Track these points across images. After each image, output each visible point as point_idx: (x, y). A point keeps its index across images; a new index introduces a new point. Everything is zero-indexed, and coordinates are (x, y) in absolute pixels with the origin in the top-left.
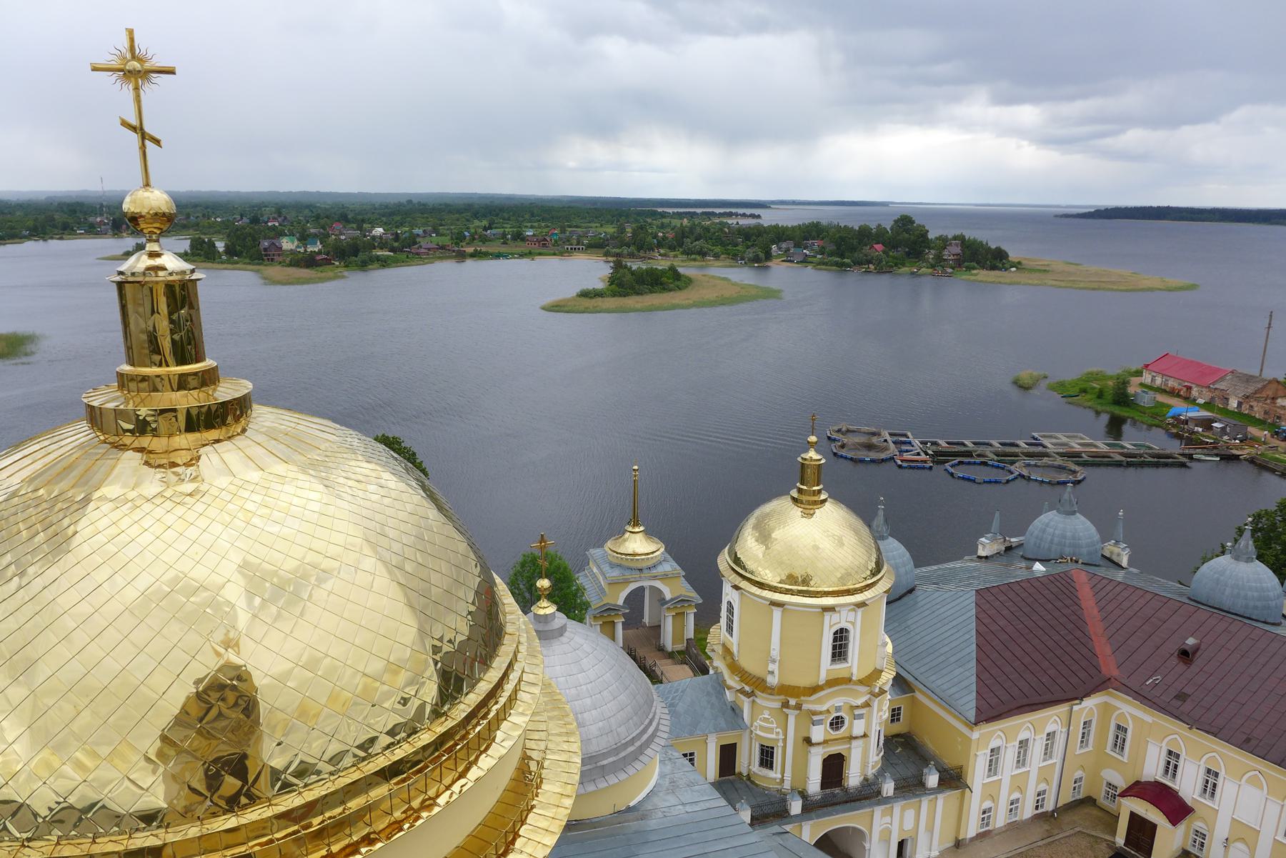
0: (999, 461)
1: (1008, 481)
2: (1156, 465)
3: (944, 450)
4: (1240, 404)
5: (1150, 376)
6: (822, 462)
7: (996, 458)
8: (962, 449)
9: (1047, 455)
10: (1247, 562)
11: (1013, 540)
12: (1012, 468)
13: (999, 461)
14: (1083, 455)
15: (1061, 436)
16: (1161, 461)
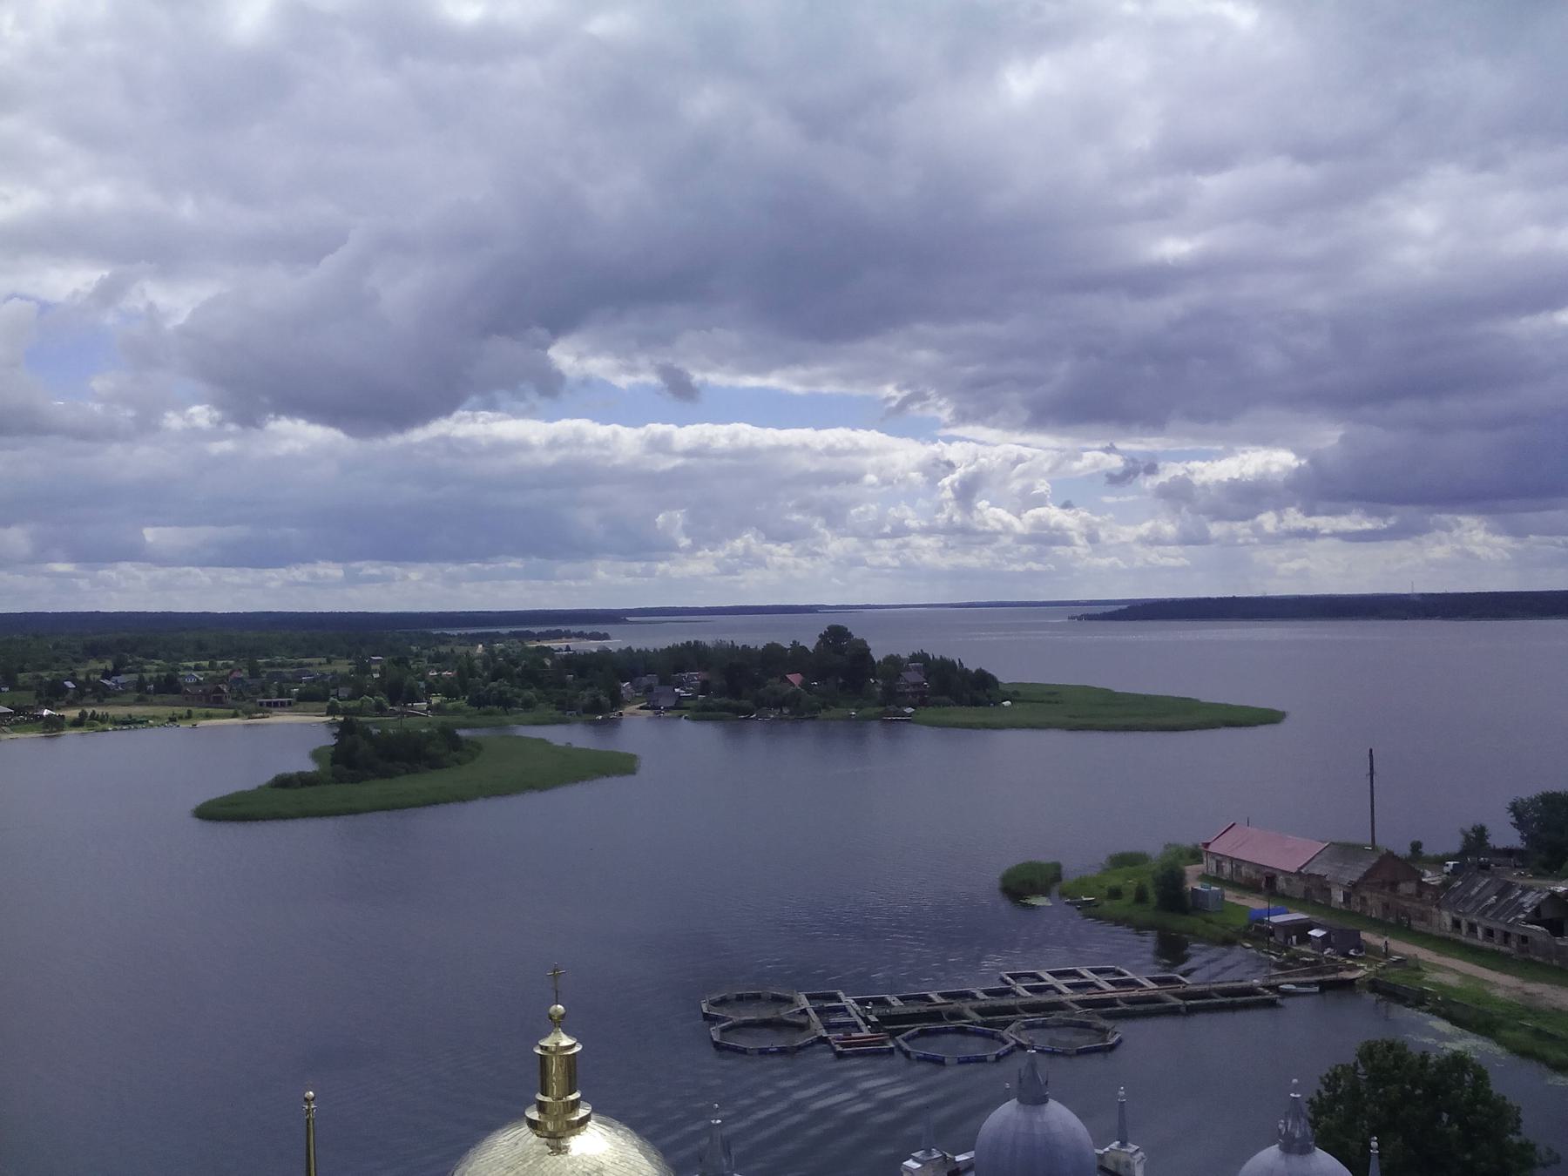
0: (985, 1024)
1: (998, 1058)
2: (1233, 1007)
3: (894, 1011)
4: (1347, 897)
5: (1214, 862)
6: (577, 1049)
7: (978, 1018)
8: (923, 1008)
9: (1059, 1006)
10: (1301, 1154)
11: (959, 1158)
12: (1005, 1034)
13: (985, 1024)
14: (1119, 1002)
15: (1085, 973)
16: (1239, 1000)
